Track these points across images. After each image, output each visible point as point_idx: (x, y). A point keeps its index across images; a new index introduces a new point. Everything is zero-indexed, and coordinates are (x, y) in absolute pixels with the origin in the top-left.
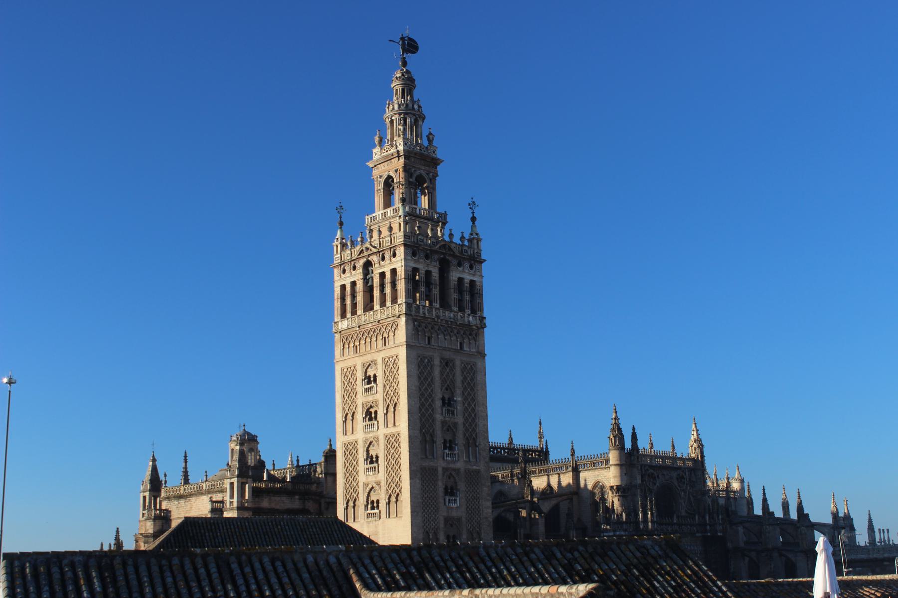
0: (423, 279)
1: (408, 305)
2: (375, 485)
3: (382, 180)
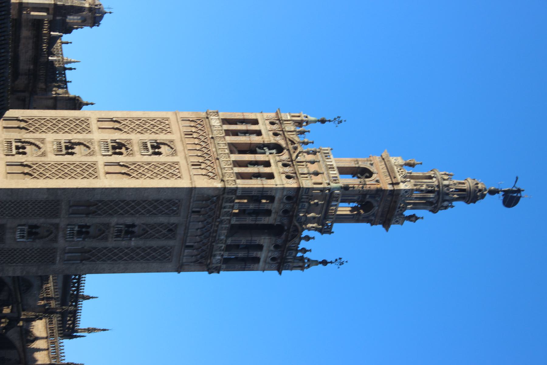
0: (262, 207)
2: (42, 150)
3: (368, 166)
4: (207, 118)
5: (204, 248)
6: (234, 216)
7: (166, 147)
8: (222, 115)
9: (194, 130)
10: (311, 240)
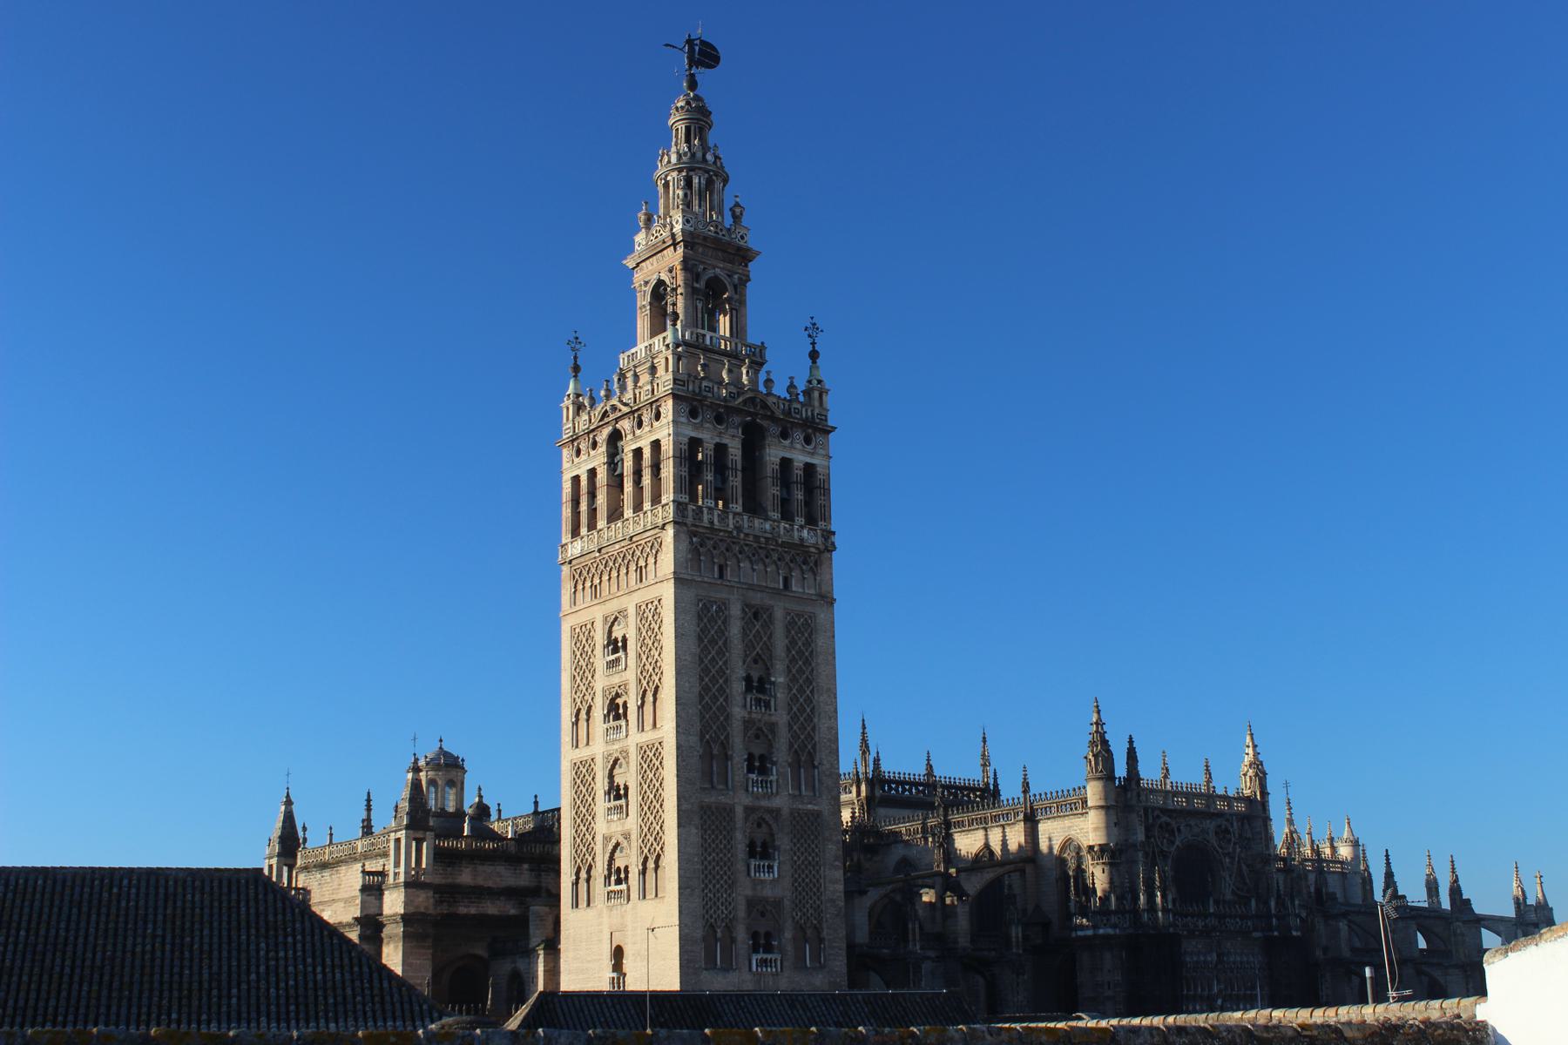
1: (679, 507)
2: (621, 839)
3: (649, 289)
5: (788, 558)
7: (615, 628)
9: (588, 584)
10: (772, 377)
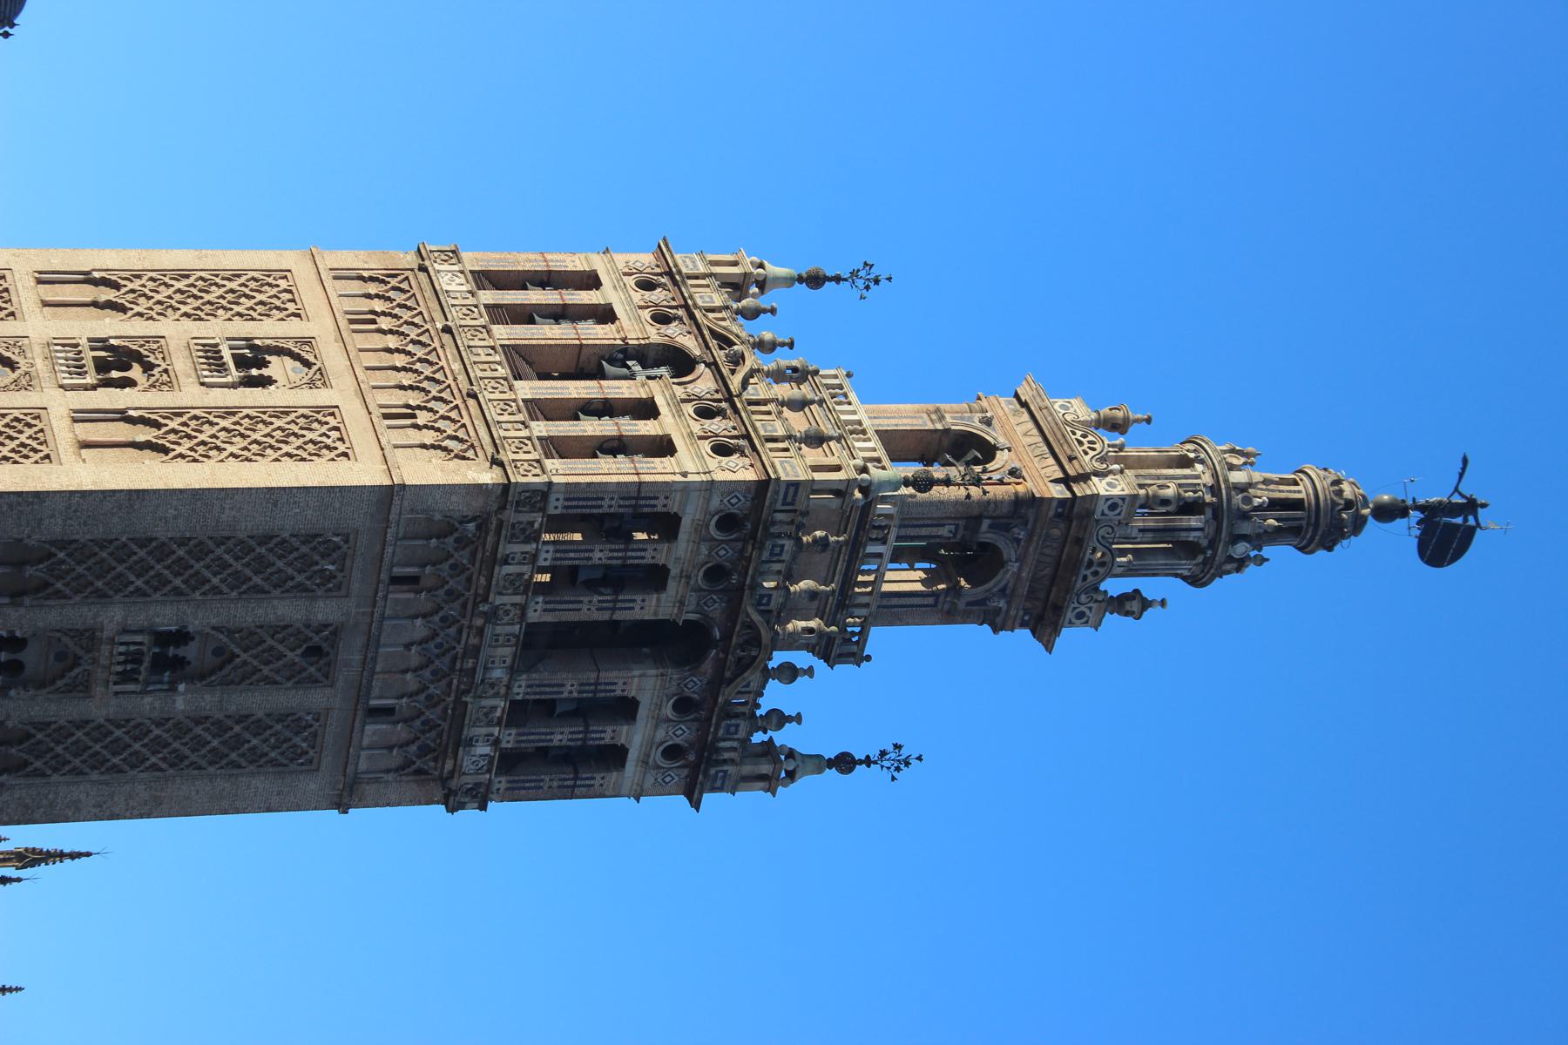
0: (634, 558)
3: (975, 426)
4: (423, 269)
5: (429, 715)
6: (536, 593)
7: (287, 360)
8: (474, 259)
9: (378, 306)
10: (802, 680)
